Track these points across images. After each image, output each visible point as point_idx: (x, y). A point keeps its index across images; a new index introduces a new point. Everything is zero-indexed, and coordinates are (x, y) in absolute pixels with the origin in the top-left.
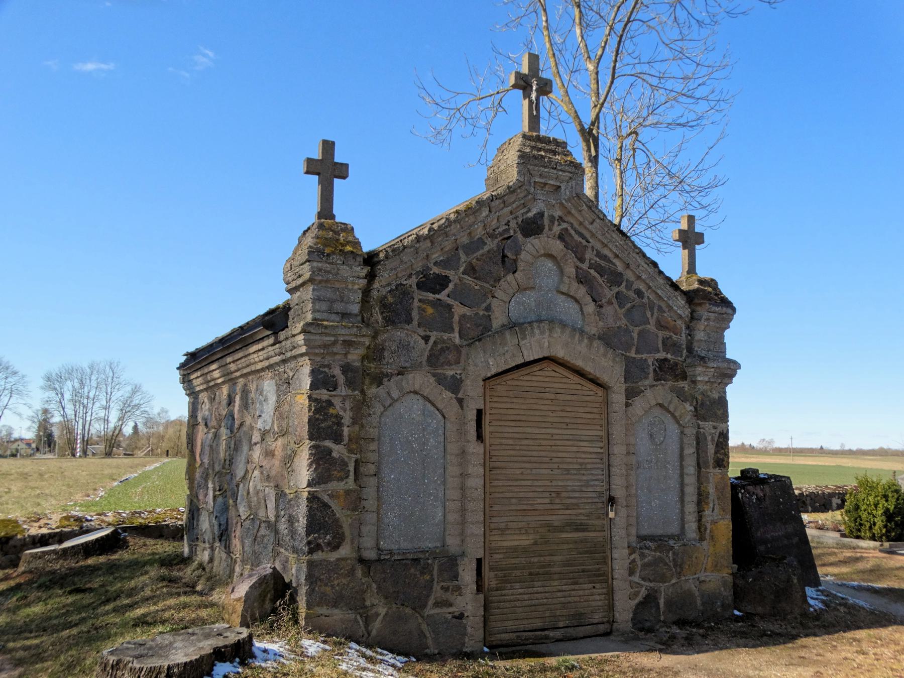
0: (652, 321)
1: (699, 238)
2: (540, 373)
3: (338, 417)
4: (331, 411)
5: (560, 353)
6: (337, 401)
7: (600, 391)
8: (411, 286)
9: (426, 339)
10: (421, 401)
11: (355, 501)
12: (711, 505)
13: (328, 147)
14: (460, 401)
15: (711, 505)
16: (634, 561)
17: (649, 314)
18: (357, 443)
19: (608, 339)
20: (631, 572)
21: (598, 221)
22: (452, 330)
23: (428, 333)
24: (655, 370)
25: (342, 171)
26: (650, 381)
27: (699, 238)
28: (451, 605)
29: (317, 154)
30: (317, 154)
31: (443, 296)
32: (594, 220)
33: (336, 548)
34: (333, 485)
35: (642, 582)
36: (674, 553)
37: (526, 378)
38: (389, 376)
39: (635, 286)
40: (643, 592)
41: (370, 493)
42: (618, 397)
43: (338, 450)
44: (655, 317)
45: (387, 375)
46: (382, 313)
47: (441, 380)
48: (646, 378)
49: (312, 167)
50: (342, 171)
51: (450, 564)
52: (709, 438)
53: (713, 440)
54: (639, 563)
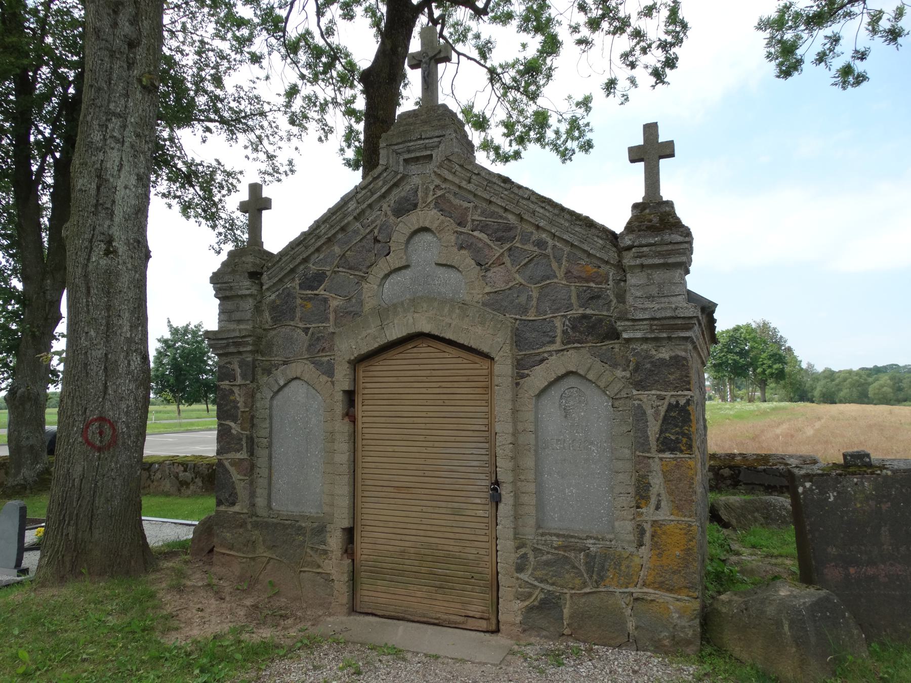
0: (560, 274)
1: (266, 204)
2: (415, 350)
3: (235, 402)
4: (232, 398)
5: (427, 329)
6: (236, 390)
7: (486, 364)
8: (294, 288)
9: (306, 330)
10: (305, 385)
11: (251, 469)
12: (653, 500)
13: (651, 130)
14: (333, 383)
15: (653, 500)
16: (524, 556)
17: (555, 265)
18: (251, 421)
19: (496, 303)
20: (520, 569)
21: (474, 177)
22: (327, 319)
23: (308, 326)
24: (564, 332)
25: (668, 150)
26: (557, 346)
27: (266, 204)
28: (319, 566)
29: (639, 141)
30: (639, 141)
31: (320, 291)
32: (470, 178)
33: (233, 504)
34: (232, 455)
35: (536, 583)
36: (587, 555)
37: (397, 357)
38: (277, 367)
39: (534, 238)
40: (538, 595)
41: (262, 462)
42: (504, 368)
43: (235, 428)
44: (563, 269)
45: (275, 366)
46: (270, 314)
47: (317, 364)
48: (553, 342)
49: (636, 154)
50: (668, 150)
51: (321, 531)
52: (650, 412)
53: (657, 413)
54: (532, 559)
